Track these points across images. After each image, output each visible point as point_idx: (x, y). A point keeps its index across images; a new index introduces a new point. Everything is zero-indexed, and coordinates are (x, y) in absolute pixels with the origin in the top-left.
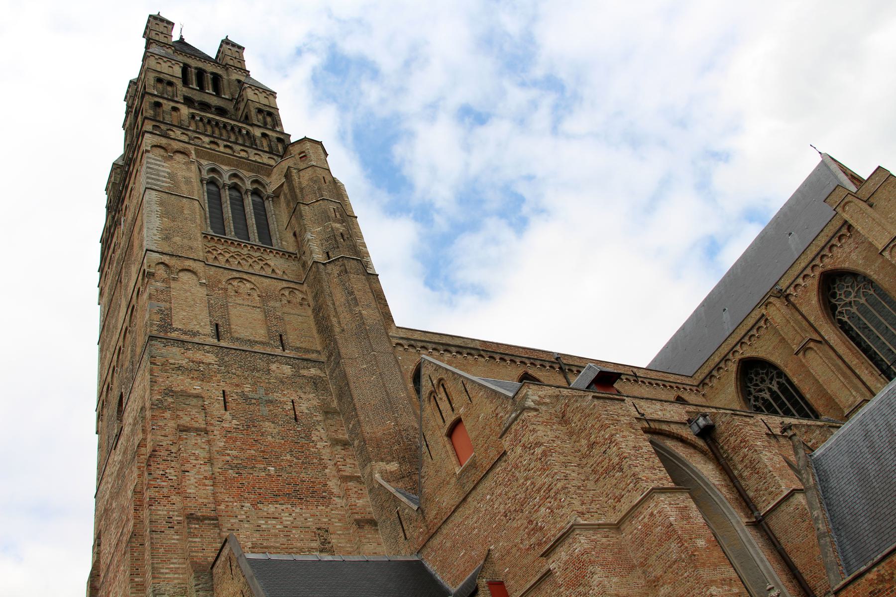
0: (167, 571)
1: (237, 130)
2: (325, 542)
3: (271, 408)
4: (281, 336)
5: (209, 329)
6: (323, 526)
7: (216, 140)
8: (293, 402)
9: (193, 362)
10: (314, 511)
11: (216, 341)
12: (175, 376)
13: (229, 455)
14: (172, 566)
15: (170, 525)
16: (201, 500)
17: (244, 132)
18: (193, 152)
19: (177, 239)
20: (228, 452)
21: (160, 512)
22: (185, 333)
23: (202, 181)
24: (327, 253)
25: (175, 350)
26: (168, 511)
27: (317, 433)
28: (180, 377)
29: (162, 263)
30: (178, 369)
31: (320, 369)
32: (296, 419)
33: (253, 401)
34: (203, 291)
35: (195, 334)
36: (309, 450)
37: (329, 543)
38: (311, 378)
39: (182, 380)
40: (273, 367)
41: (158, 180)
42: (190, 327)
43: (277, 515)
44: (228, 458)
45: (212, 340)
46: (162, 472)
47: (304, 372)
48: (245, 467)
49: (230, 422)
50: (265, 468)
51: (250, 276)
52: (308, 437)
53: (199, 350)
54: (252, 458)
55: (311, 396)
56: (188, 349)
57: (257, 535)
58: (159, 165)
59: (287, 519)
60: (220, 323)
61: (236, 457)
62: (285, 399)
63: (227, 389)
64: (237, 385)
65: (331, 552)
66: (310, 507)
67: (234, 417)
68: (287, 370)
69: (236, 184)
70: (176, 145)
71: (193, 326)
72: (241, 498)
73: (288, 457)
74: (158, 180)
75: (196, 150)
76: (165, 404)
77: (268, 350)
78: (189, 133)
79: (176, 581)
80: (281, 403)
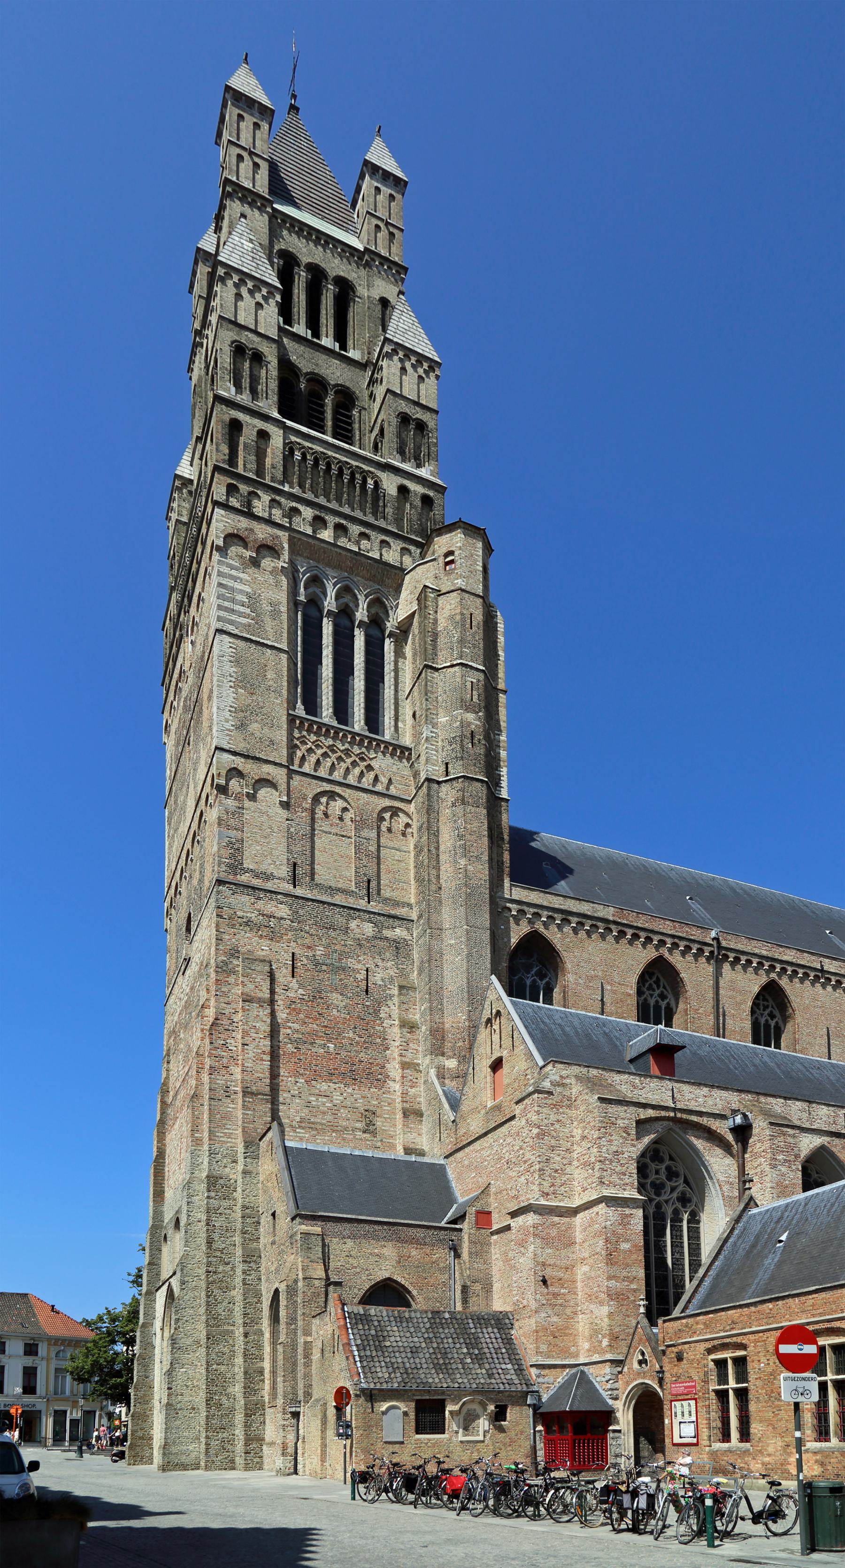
3: (343, 976)
5: (284, 871)
6: (371, 1108)
8: (367, 970)
11: (291, 887)
13: (290, 1028)
20: (290, 1024)
22: (257, 876)
30: (247, 924)
32: (367, 991)
33: (324, 967)
35: (268, 877)
36: (374, 1028)
37: (374, 1125)
38: (394, 941)
40: (353, 924)
42: (263, 868)
43: (328, 1094)
44: (289, 1031)
50: (325, 1045)
52: (376, 1012)
54: (314, 1033)
55: (389, 964)
56: (259, 898)
59: (337, 1098)
60: (299, 862)
61: (297, 1031)
62: (360, 966)
63: (297, 951)
64: (309, 947)
67: (301, 986)
68: (368, 929)
71: (267, 866)
73: (351, 1035)
77: (351, 902)
80: (354, 970)
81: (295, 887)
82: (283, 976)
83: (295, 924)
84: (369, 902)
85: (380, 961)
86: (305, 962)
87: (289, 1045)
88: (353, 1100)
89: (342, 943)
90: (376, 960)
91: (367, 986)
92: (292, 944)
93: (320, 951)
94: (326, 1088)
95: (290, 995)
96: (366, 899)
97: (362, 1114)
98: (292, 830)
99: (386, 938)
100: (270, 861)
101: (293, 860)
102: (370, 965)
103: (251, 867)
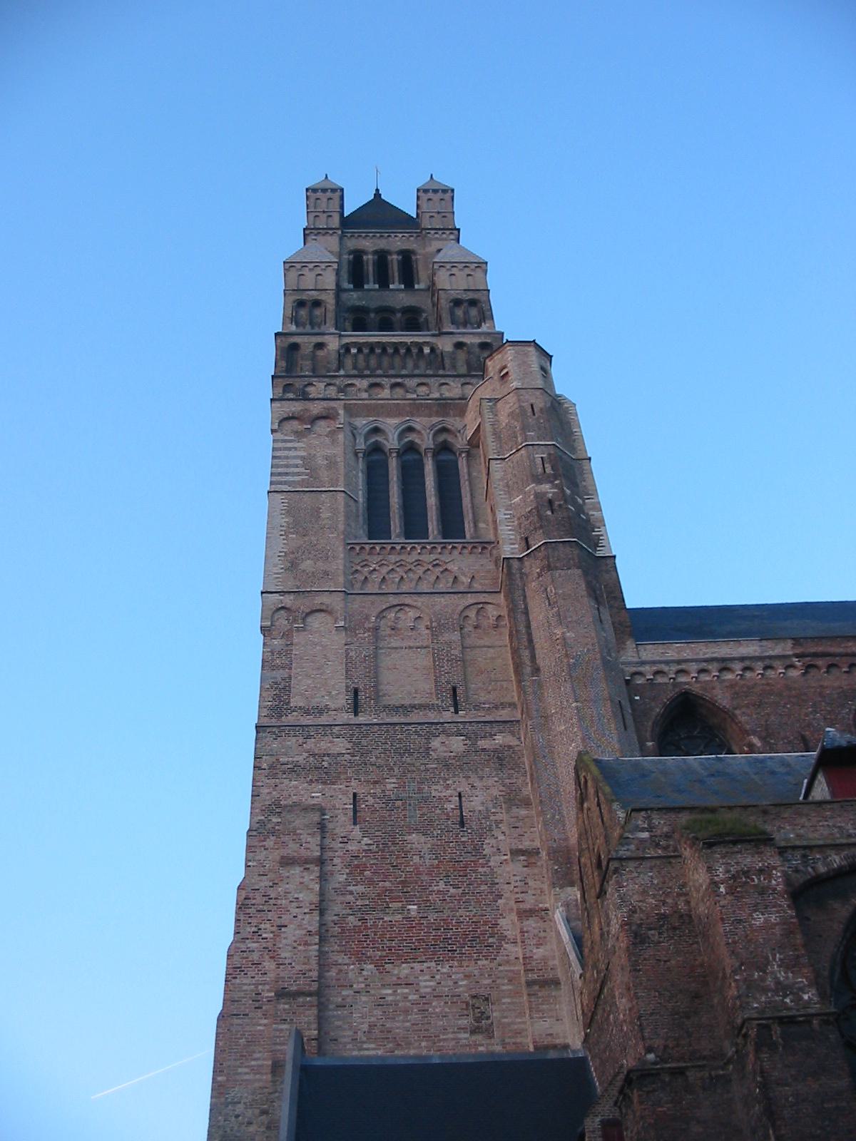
0: (246, 1070)
1: (415, 351)
2: (482, 1016)
3: (425, 810)
4: (454, 689)
5: (343, 700)
6: (482, 992)
7: (378, 380)
8: (460, 796)
9: (314, 755)
10: (472, 969)
11: (352, 716)
12: (286, 781)
13: (351, 893)
14: (253, 1063)
15: (257, 1004)
16: (298, 968)
17: (427, 350)
18: (341, 412)
19: (307, 565)
21: (245, 988)
22: (307, 712)
23: (356, 454)
24: (526, 539)
25: (292, 742)
26: (256, 985)
27: (493, 841)
28: (293, 783)
29: (283, 608)
30: (292, 770)
31: (512, 733)
32: (462, 824)
33: (399, 803)
34: (341, 638)
35: (321, 711)
37: (488, 1018)
38: (495, 751)
39: (296, 787)
40: (435, 743)
41: (287, 474)
42: (314, 702)
43: (412, 980)
44: (350, 898)
45: (346, 716)
46: (254, 929)
47: (482, 743)
48: (374, 909)
49: (359, 841)
50: (403, 908)
51: (415, 597)
52: (477, 850)
53: (325, 735)
55: (490, 782)
56: (309, 737)
57: (378, 1012)
58: (290, 449)
59: (426, 984)
61: (362, 896)
62: (449, 792)
63: (361, 791)
64: (376, 782)
65: (489, 1032)
66: (465, 964)
67: (365, 833)
69: (412, 442)
70: (316, 408)
71: (321, 699)
72: (361, 958)
73: (442, 886)
74: (287, 474)
75: (346, 407)
76: (269, 826)
77: (432, 716)
78: (337, 381)
79: (257, 1085)
80: (440, 798)
81: (356, 714)
82: (341, 823)
83: (358, 758)
84: (456, 712)
85: (477, 780)
86: (371, 801)
87: (351, 918)
88: (450, 983)
89: (422, 768)
90: (471, 781)
91: (462, 816)
92: (354, 783)
93: (391, 784)
94: (406, 971)
95: (350, 848)
96: (452, 709)
97: (467, 1004)
98: (352, 654)
99: (484, 750)
100: (324, 693)
101: (353, 685)
102: (464, 787)
103: (301, 704)
